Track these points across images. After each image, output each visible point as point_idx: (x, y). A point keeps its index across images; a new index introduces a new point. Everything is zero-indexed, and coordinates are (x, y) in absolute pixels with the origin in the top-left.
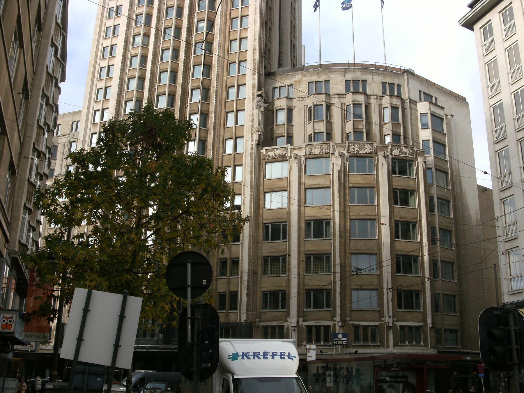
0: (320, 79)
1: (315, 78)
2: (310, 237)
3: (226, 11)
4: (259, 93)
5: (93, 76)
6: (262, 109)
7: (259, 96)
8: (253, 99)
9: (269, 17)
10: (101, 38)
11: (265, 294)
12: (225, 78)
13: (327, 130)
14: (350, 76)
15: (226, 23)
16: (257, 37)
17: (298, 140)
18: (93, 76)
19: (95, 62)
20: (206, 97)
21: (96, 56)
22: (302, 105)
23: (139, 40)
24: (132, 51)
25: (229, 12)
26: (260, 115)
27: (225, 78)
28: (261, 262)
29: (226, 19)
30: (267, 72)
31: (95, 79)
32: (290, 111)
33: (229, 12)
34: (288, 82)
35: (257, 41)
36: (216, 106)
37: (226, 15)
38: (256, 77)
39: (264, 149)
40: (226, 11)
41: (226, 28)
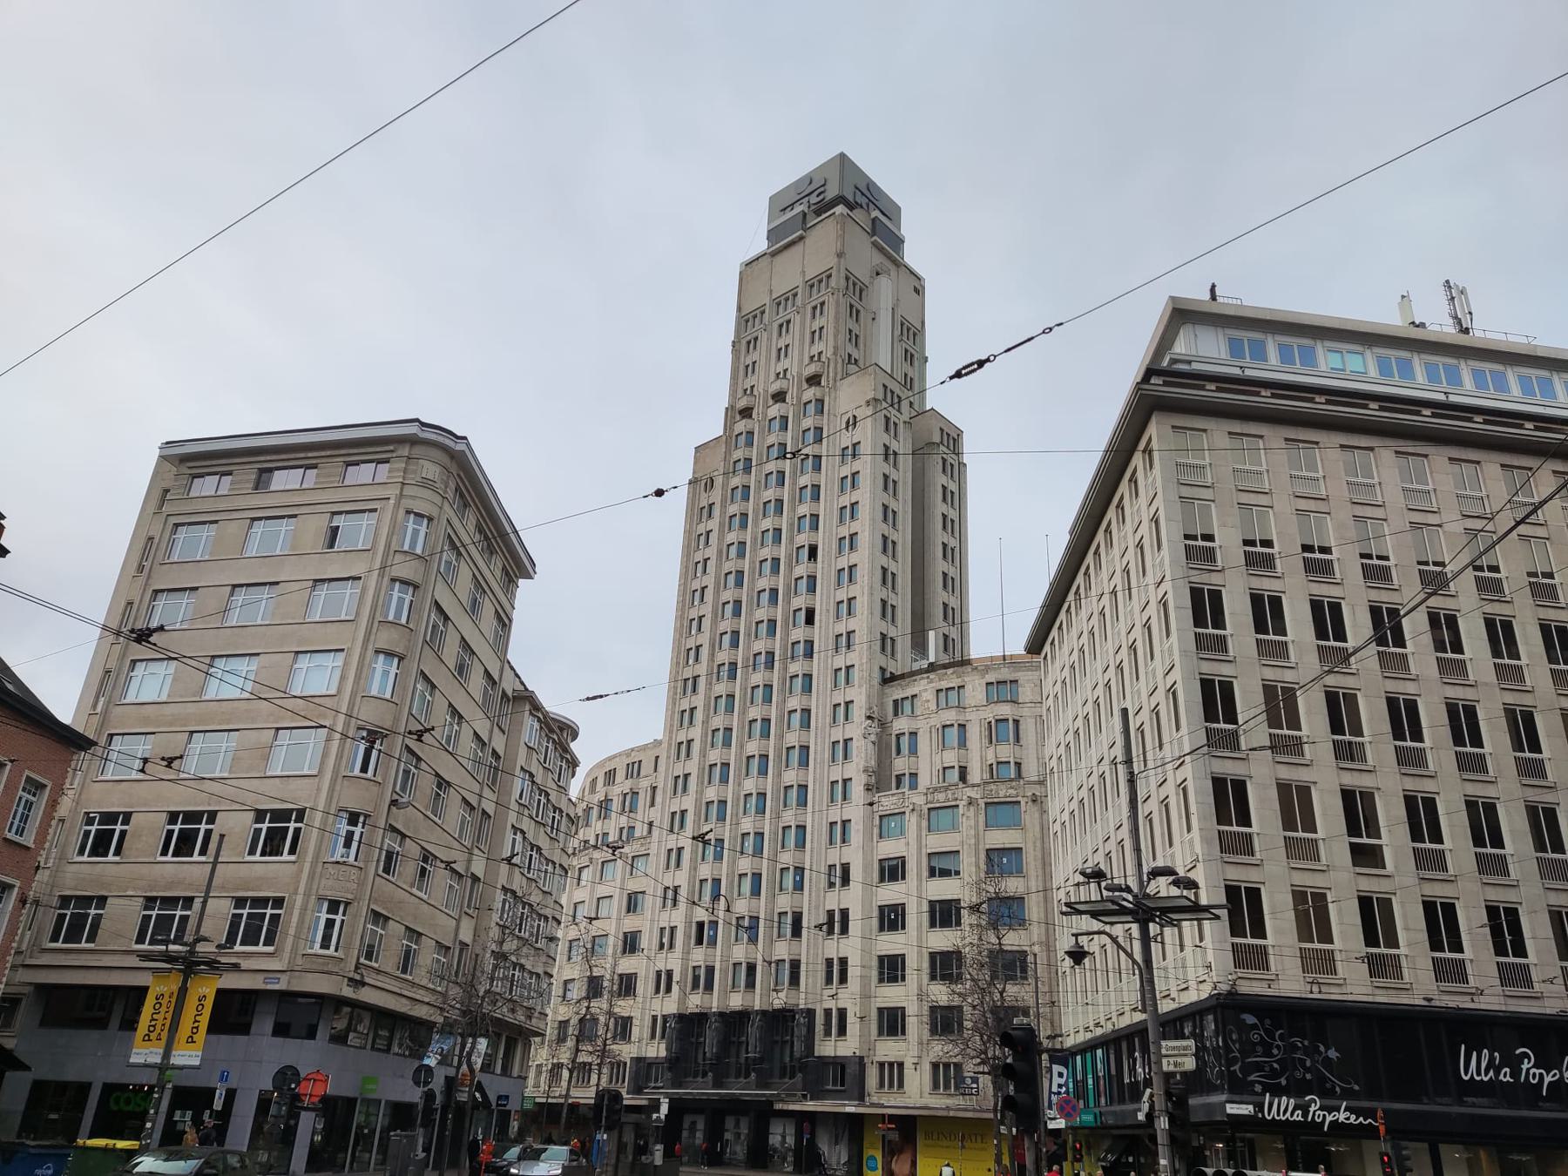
0: (951, 685)
1: (944, 684)
2: (936, 927)
6: (873, 738)
7: (869, 718)
11: (880, 1010)
14: (991, 677)
17: (924, 781)
26: (870, 746)
28: (875, 963)
34: (909, 692)
39: (877, 795)
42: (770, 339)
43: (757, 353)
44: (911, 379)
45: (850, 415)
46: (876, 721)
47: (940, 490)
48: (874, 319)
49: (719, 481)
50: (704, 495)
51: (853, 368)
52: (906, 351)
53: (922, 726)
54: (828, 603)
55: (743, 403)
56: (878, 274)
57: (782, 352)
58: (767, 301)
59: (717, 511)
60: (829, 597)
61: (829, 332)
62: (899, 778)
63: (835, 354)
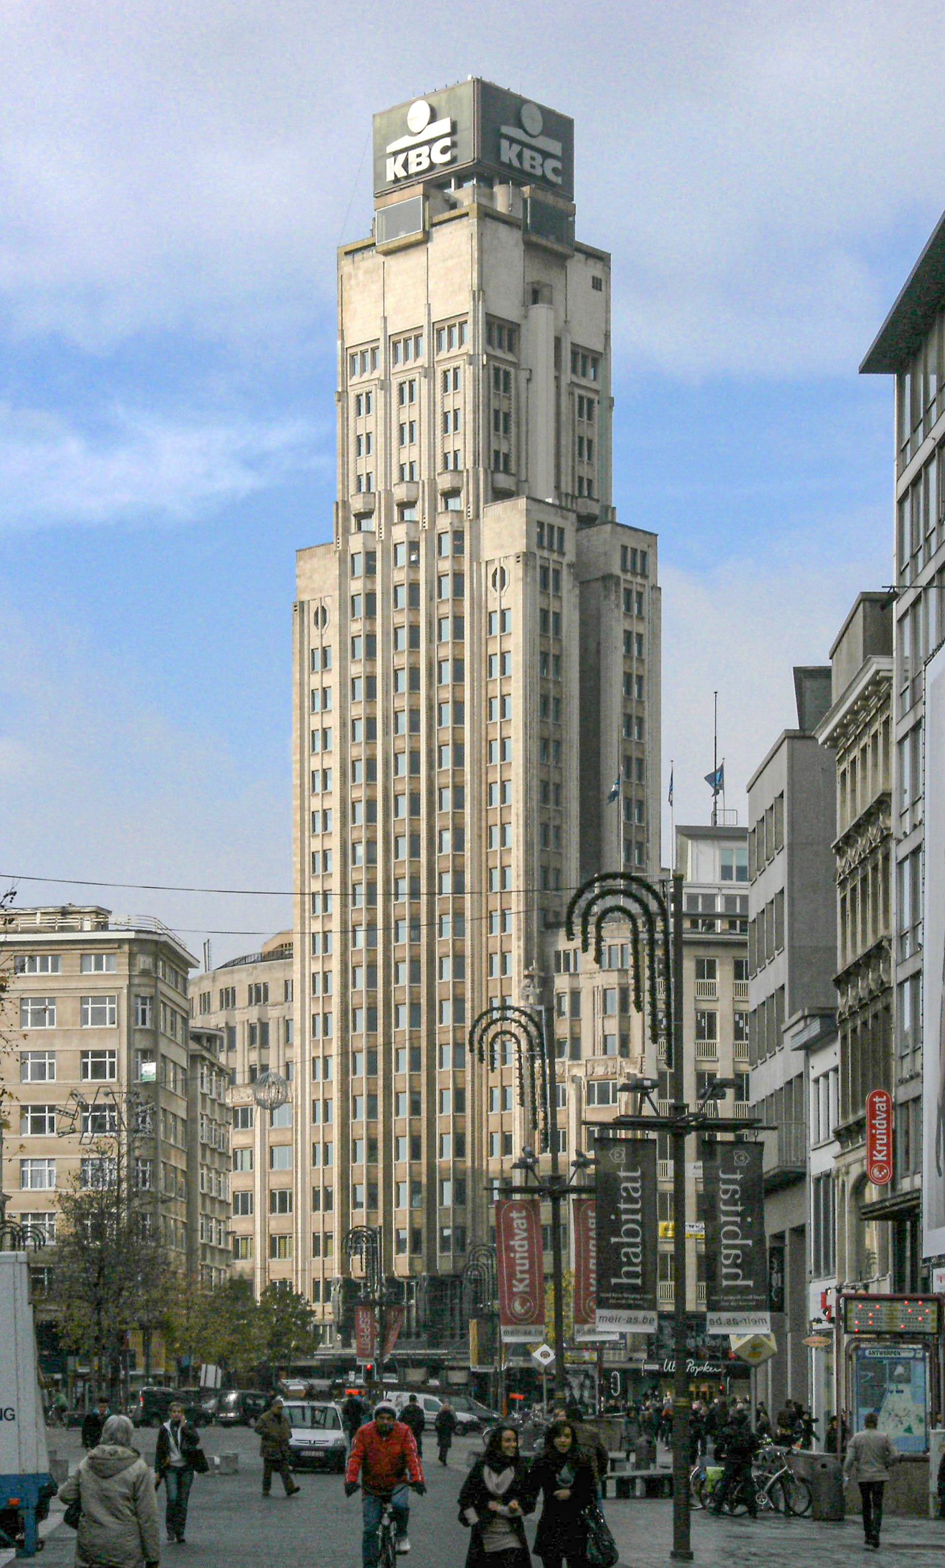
3: (480, 811)
4: (526, 973)
5: (303, 910)
7: (526, 977)
8: (519, 981)
9: (551, 806)
10: (307, 834)
12: (484, 939)
13: (620, 1030)
15: (480, 837)
16: (522, 872)
18: (303, 910)
19: (303, 883)
20: (459, 971)
21: (302, 871)
22: (590, 988)
23: (361, 850)
24: (353, 876)
25: (484, 814)
27: (484, 939)
29: (480, 828)
30: (551, 919)
31: (307, 914)
32: (575, 995)
33: (484, 814)
35: (521, 878)
36: (473, 989)
37: (480, 819)
38: (522, 943)
40: (480, 811)
41: (481, 847)
42: (387, 405)
43: (371, 419)
44: (581, 454)
45: (496, 565)
46: (536, 980)
47: (621, 636)
48: (529, 380)
49: (334, 617)
50: (315, 631)
51: (503, 481)
52: (581, 398)
53: (585, 985)
54: (480, 828)
55: (357, 504)
56: (535, 295)
57: (406, 432)
58: (379, 334)
59: (334, 663)
60: (480, 819)
61: (467, 419)
62: (561, 1044)
63: (476, 462)
